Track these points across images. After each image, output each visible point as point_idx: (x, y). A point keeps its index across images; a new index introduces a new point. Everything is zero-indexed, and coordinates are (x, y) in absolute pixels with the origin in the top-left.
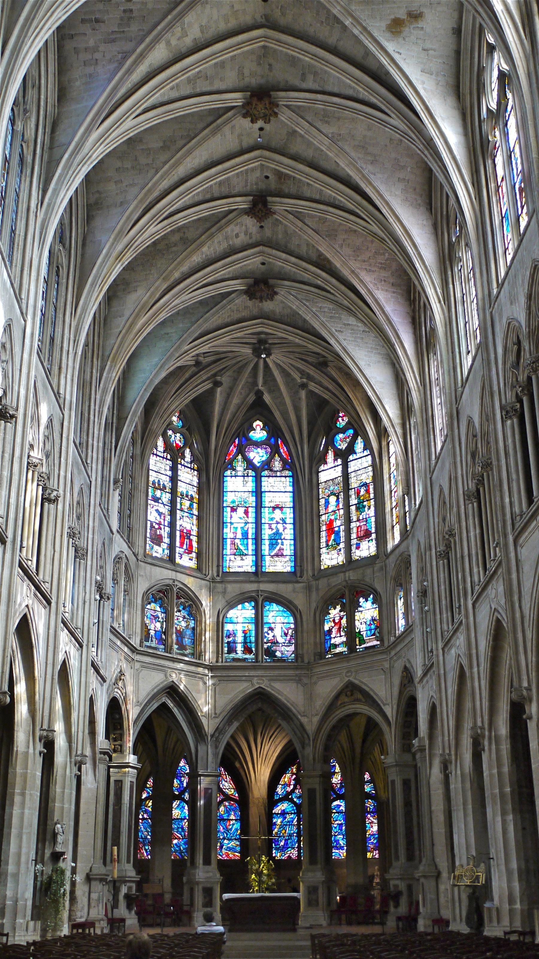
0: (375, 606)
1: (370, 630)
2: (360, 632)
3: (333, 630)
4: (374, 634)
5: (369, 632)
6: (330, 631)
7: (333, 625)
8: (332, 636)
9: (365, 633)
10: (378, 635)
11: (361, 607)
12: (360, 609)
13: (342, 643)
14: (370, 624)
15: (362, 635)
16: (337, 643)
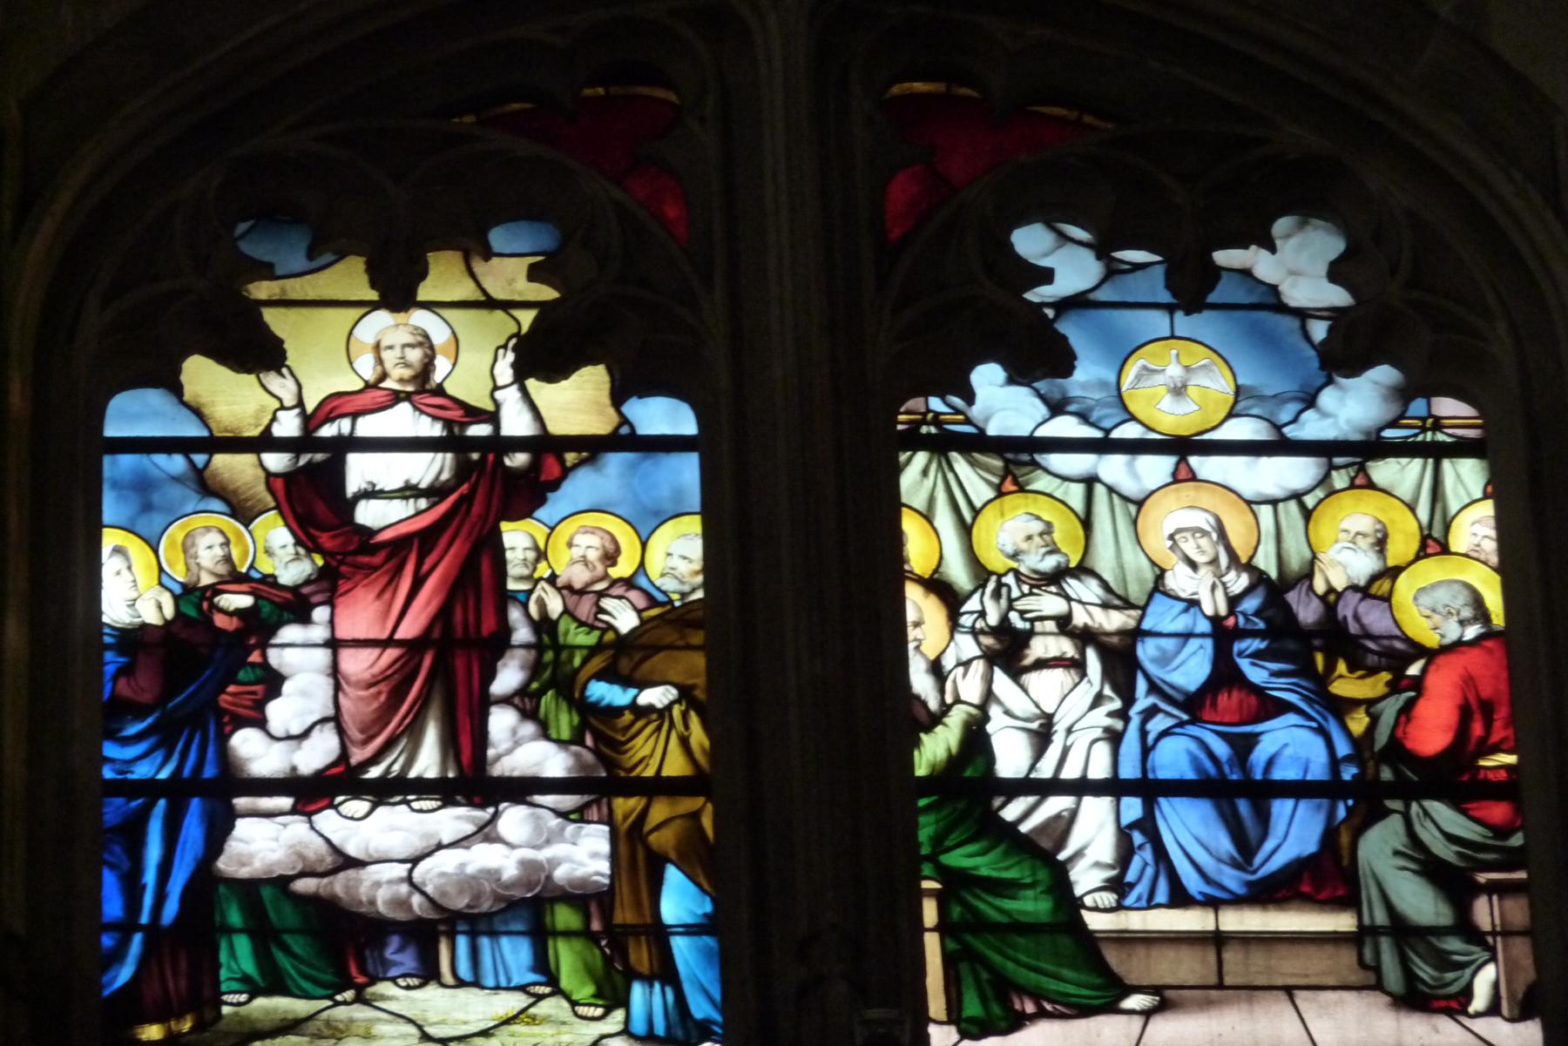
0: (1353, 405)
1: (1239, 794)
2: (971, 780)
3: (298, 654)
4: (1327, 876)
5: (1190, 829)
6: (210, 662)
7: (278, 552)
8: (255, 751)
9: (1094, 831)
10: (1421, 903)
11: (1039, 357)
12: (1001, 402)
13: (531, 907)
14: (1221, 697)
15: (1045, 855)
16: (379, 887)
